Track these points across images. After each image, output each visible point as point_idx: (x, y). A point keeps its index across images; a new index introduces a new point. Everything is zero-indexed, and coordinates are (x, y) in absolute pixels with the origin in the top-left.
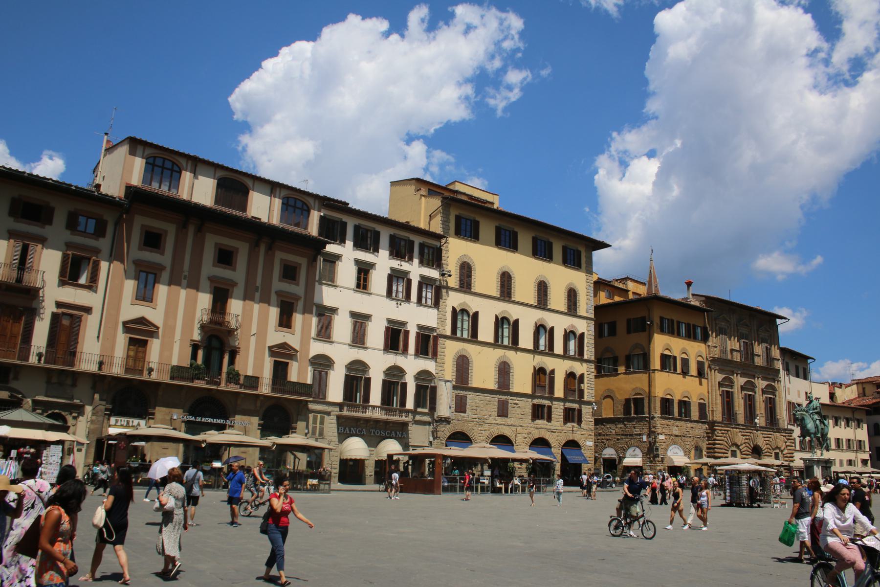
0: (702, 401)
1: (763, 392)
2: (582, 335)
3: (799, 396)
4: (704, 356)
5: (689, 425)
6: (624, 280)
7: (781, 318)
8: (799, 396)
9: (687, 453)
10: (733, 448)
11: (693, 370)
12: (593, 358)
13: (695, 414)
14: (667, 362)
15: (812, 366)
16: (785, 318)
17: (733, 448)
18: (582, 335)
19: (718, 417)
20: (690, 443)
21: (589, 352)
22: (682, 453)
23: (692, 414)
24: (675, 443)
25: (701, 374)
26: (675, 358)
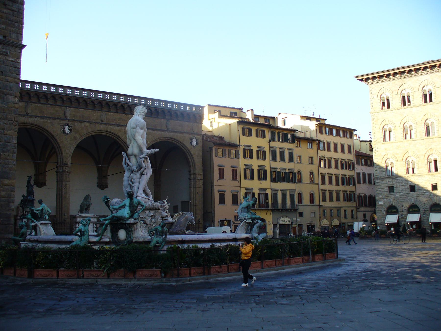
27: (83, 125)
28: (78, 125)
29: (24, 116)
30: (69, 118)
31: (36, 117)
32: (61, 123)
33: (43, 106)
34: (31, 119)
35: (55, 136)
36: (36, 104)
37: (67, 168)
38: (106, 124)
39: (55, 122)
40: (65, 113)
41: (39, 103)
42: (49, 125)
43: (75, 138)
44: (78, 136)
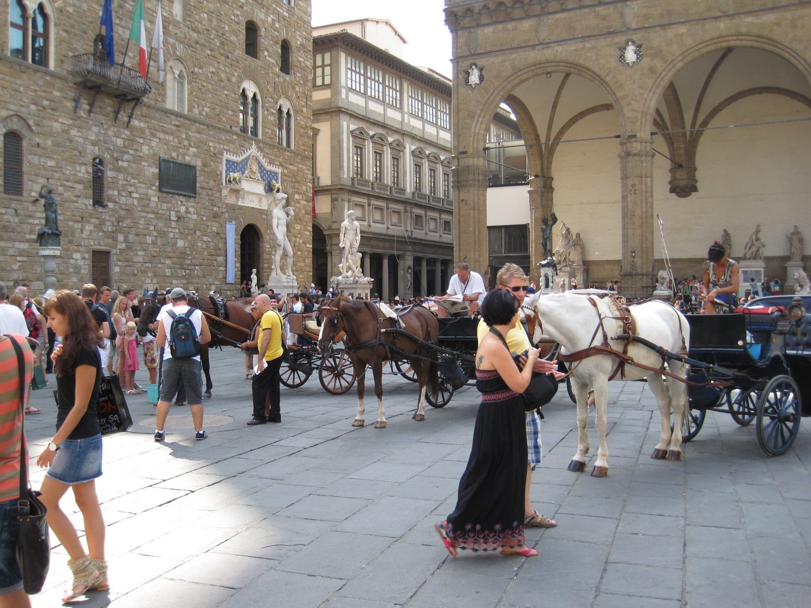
27: (671, 33)
28: (656, 39)
29: (533, 46)
30: (634, 26)
31: (559, 42)
32: (616, 44)
33: (572, 14)
34: (550, 51)
35: (603, 75)
36: (558, 16)
37: (635, 144)
38: (732, 16)
39: (602, 42)
40: (622, 15)
41: (564, 10)
42: (589, 54)
43: (652, 70)
44: (659, 65)
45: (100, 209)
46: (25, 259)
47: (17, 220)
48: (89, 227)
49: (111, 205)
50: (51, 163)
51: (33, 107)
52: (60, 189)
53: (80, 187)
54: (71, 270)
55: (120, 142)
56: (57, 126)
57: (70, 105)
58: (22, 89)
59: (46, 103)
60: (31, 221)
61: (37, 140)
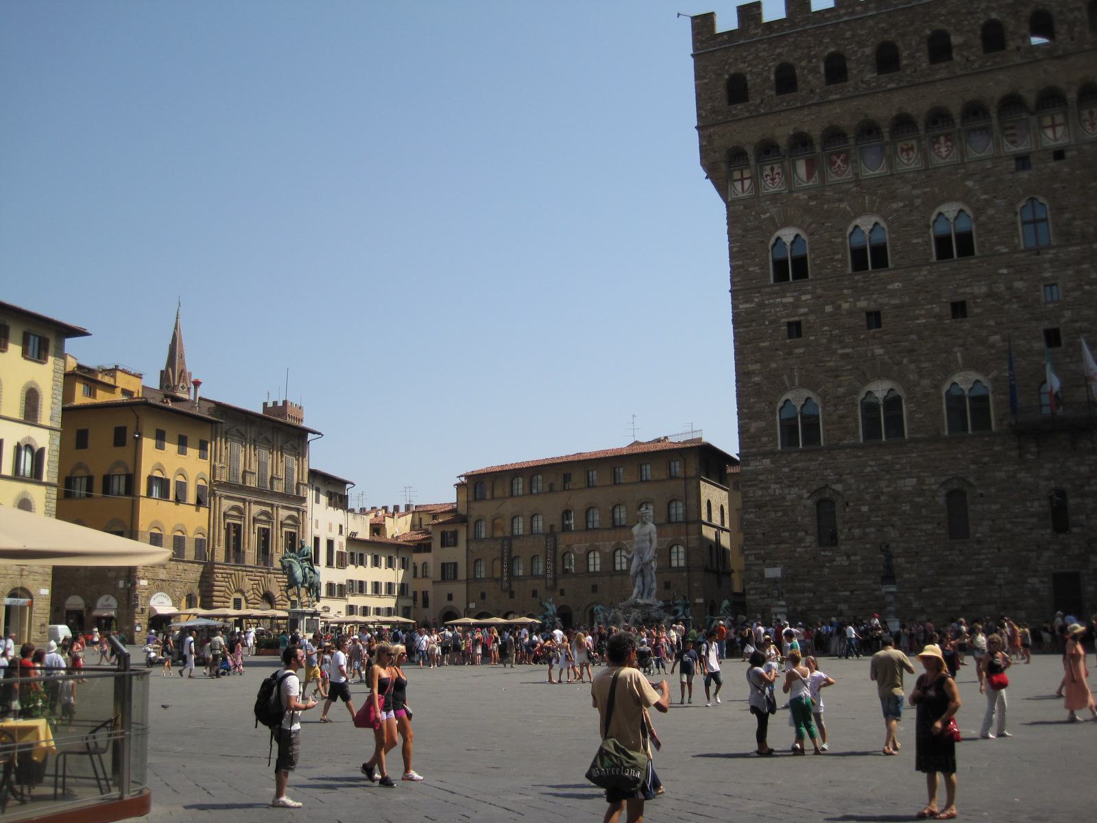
0: (200, 536)
1: (282, 525)
2: (42, 450)
3: (330, 530)
4: (208, 479)
5: (181, 566)
6: (112, 372)
7: (314, 432)
8: (330, 530)
9: (176, 603)
10: (238, 596)
11: (191, 496)
12: (55, 481)
13: (190, 552)
14: (161, 486)
15: (351, 492)
16: (319, 434)
17: (238, 596)
18: (42, 450)
19: (220, 555)
20: (181, 590)
21: (49, 471)
22: (170, 602)
23: (186, 553)
24: (161, 589)
25: (199, 503)
26: (168, 481)
45: (1061, 536)
46: (973, 588)
47: (962, 558)
48: (1047, 554)
49: (1075, 530)
50: (995, 507)
51: (972, 467)
52: (1009, 526)
53: (1034, 520)
54: (1026, 593)
55: (1084, 469)
56: (1001, 475)
57: (1014, 453)
58: (960, 456)
59: (985, 459)
60: (977, 557)
61: (979, 491)
